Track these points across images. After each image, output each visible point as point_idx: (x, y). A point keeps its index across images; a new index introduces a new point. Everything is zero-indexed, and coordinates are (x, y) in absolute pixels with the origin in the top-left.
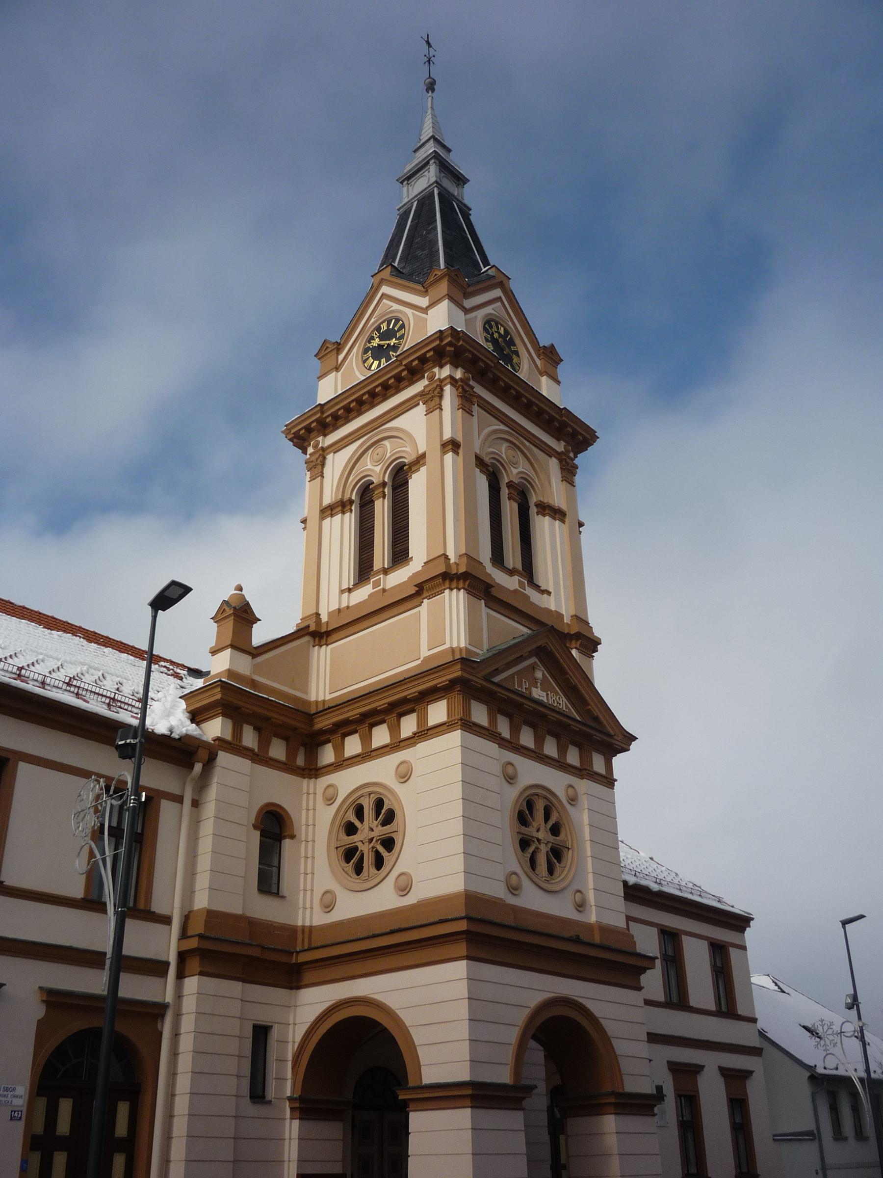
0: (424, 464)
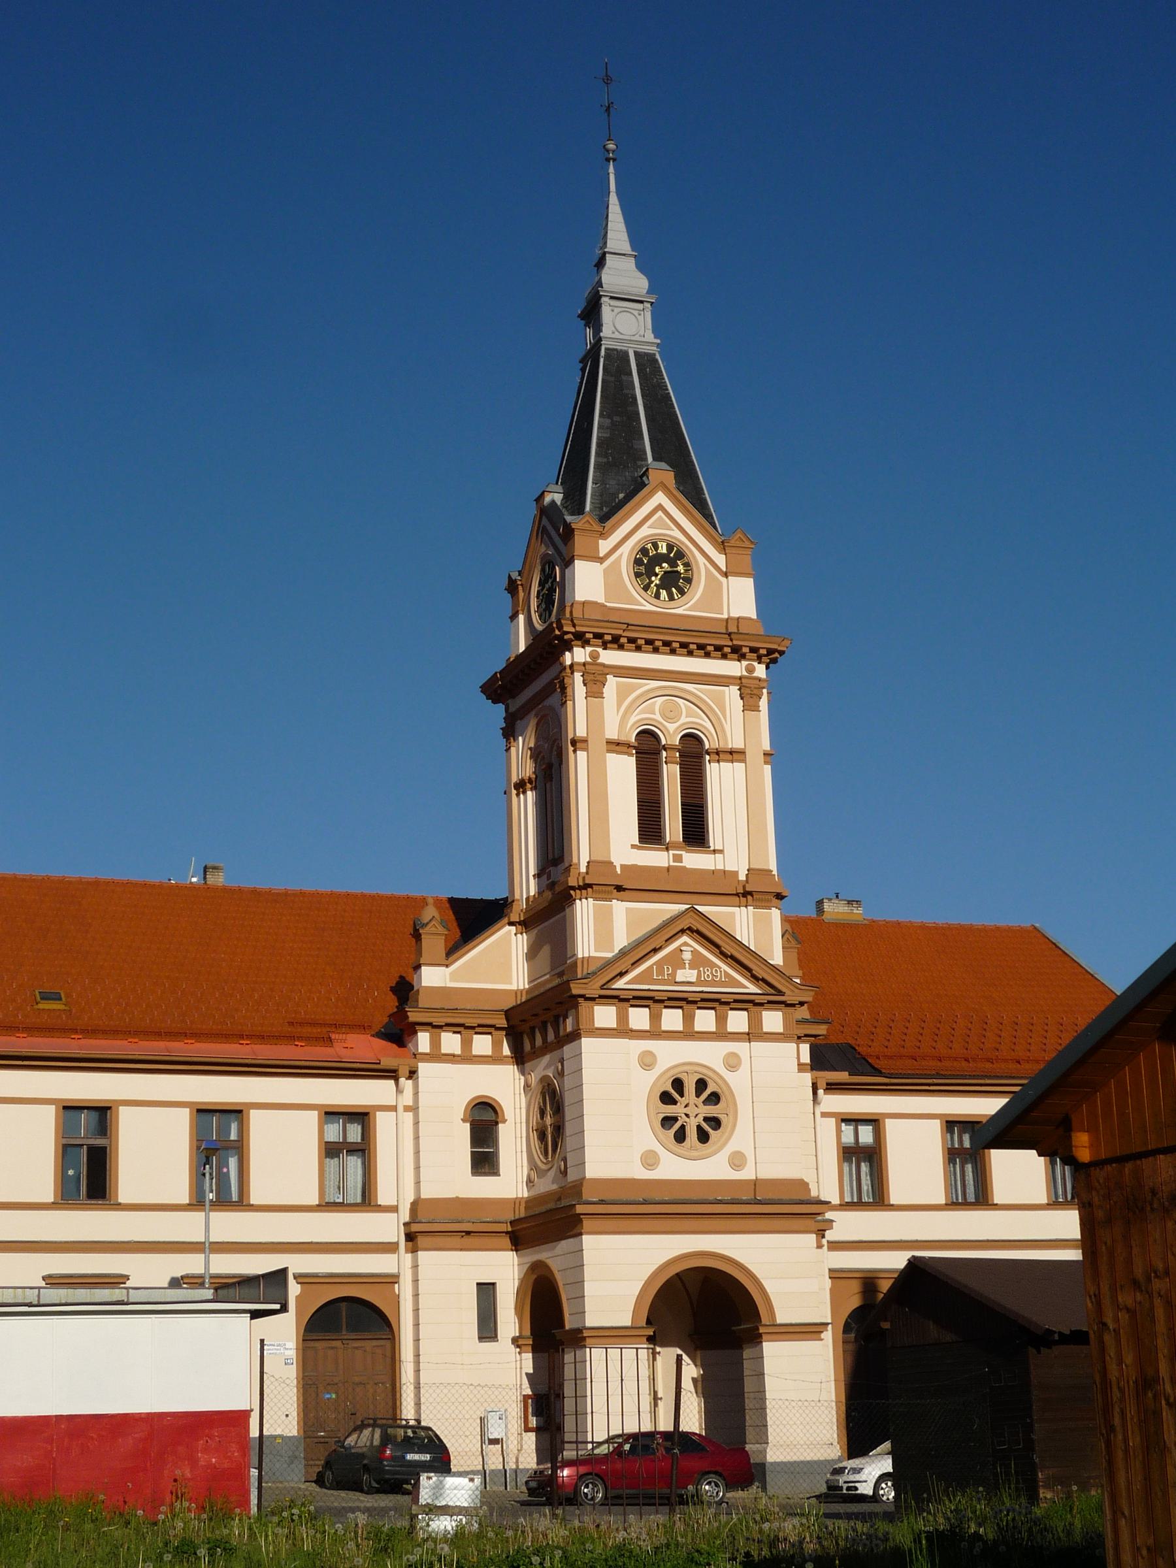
0: (744, 761)
